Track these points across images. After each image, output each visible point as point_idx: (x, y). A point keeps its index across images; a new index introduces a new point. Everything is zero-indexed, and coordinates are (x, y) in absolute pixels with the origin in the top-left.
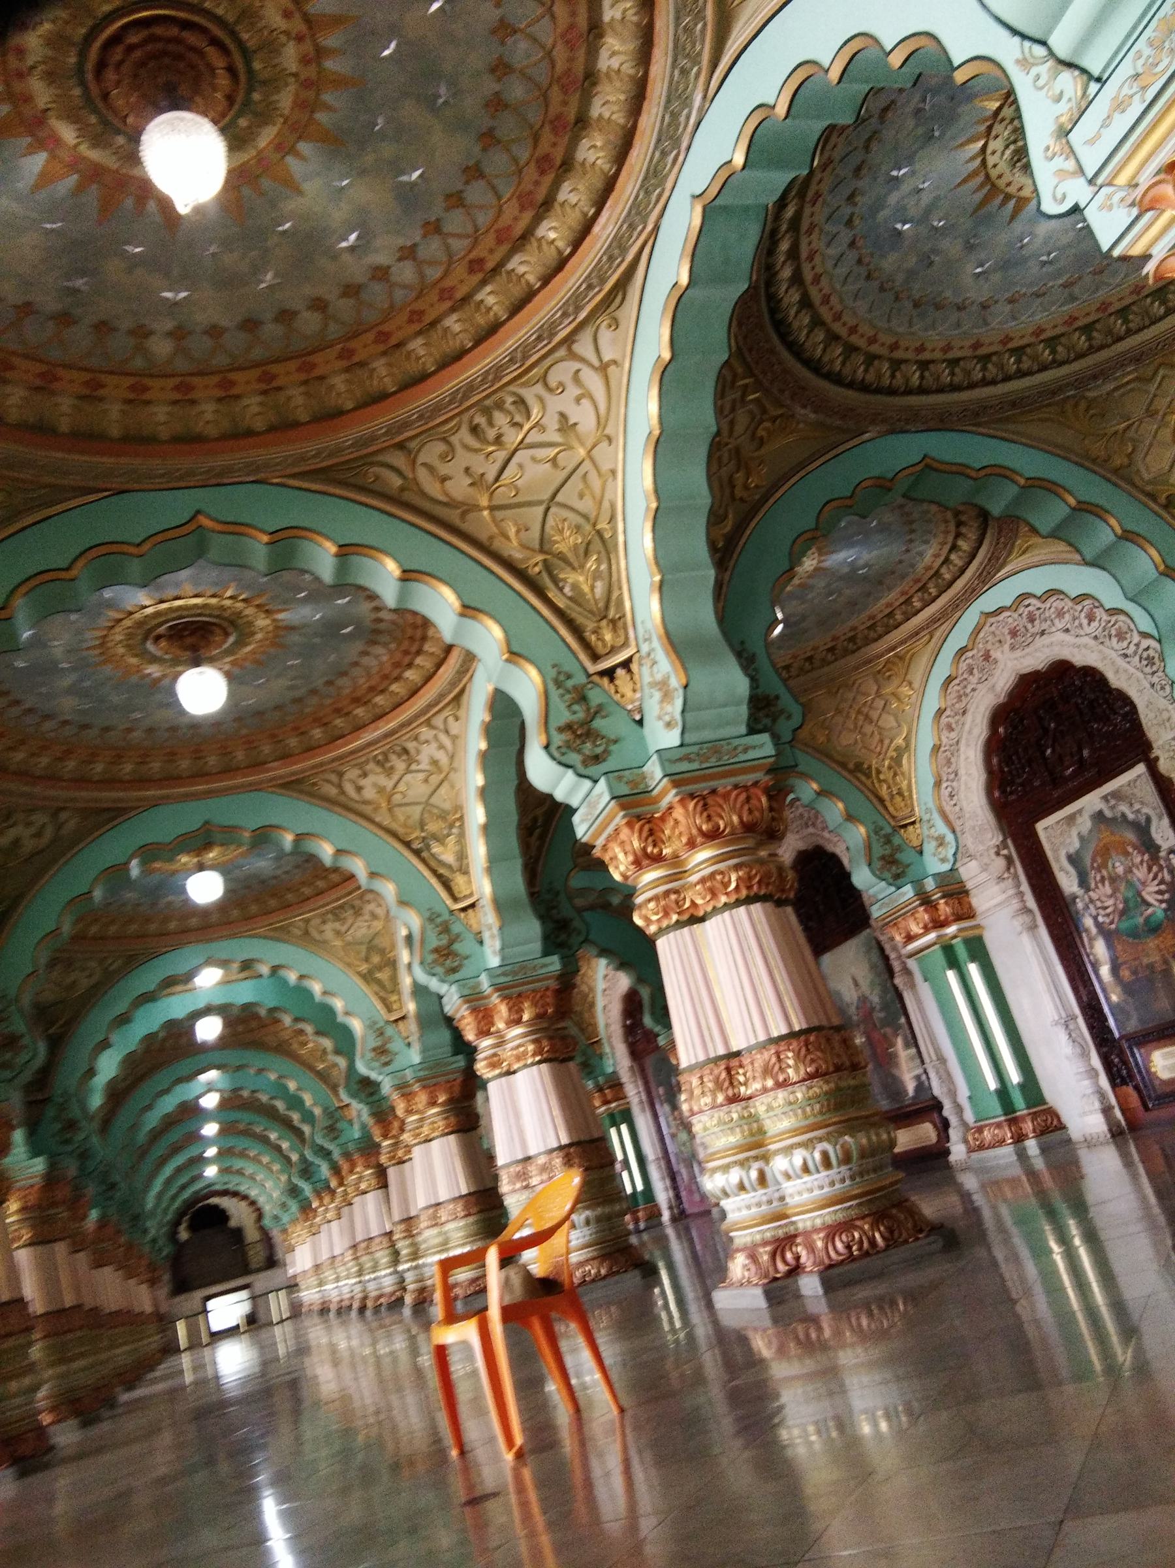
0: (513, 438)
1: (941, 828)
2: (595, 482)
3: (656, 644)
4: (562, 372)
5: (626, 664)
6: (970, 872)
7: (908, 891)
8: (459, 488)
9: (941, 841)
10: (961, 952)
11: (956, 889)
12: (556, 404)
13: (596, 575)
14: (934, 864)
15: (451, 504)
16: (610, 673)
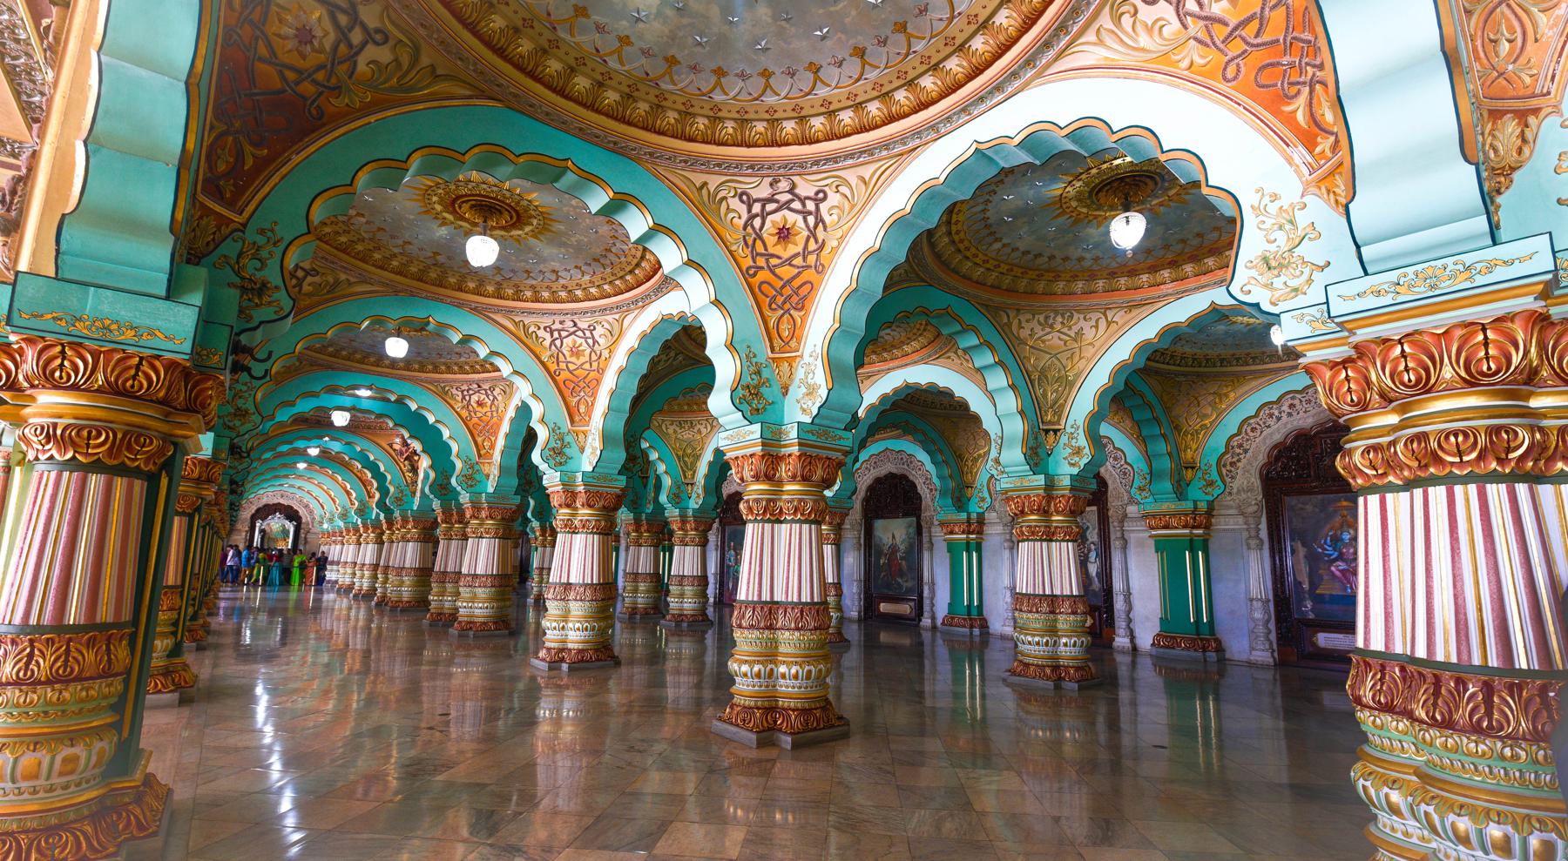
0: (1058, 327)
1: (986, 495)
2: (1076, 358)
3: (1081, 431)
4: (1094, 316)
5: (1055, 431)
6: (991, 516)
7: (964, 516)
8: (1024, 333)
9: (983, 500)
10: (973, 546)
11: (981, 521)
12: (1082, 323)
13: (1056, 391)
14: (974, 508)
15: (1018, 338)
16: (1047, 431)
